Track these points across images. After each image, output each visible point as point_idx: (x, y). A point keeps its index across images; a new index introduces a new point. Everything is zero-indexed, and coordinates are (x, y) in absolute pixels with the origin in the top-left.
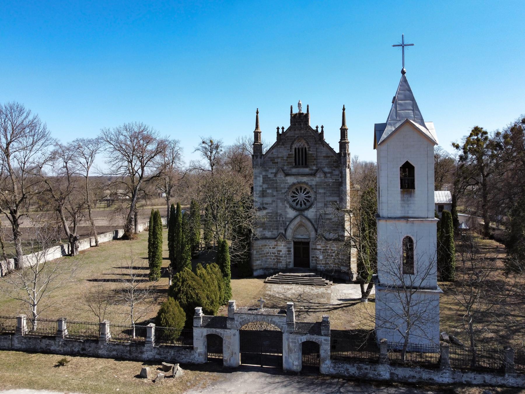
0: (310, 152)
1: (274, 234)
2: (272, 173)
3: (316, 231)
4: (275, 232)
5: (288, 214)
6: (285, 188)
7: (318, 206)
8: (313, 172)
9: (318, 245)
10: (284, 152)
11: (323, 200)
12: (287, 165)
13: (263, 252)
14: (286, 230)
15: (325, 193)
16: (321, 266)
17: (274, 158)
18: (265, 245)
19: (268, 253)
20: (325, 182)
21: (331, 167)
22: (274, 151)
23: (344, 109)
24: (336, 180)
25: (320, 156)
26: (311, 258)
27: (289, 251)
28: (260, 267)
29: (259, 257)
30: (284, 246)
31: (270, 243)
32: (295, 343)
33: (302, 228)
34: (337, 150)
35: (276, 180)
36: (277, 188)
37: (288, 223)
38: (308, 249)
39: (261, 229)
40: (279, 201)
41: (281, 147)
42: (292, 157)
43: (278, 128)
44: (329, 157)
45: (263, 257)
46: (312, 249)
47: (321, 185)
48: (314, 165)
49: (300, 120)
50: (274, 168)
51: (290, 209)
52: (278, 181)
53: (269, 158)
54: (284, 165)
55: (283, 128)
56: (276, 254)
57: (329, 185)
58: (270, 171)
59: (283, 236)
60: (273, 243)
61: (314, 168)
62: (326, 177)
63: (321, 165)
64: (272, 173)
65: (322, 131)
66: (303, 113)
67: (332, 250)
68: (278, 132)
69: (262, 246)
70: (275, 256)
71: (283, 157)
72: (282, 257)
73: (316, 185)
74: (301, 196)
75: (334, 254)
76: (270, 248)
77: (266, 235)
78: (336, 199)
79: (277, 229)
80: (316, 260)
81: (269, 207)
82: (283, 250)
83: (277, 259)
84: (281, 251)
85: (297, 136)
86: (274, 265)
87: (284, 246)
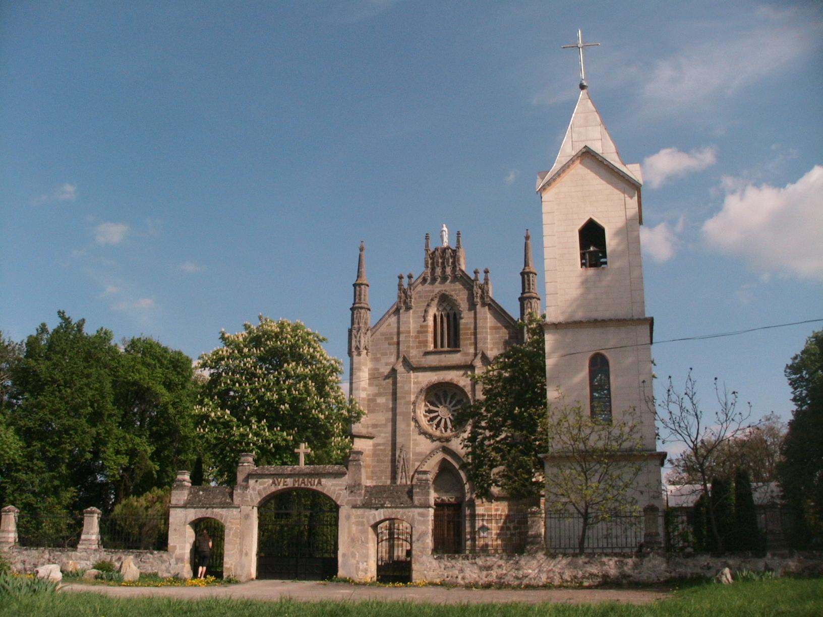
2: (387, 364)
32: (362, 524)
43: (401, 277)
48: (471, 344)
49: (442, 262)
53: (382, 334)
55: (410, 277)
58: (384, 360)
64: (387, 364)
65: (486, 280)
66: (448, 248)
68: (400, 285)
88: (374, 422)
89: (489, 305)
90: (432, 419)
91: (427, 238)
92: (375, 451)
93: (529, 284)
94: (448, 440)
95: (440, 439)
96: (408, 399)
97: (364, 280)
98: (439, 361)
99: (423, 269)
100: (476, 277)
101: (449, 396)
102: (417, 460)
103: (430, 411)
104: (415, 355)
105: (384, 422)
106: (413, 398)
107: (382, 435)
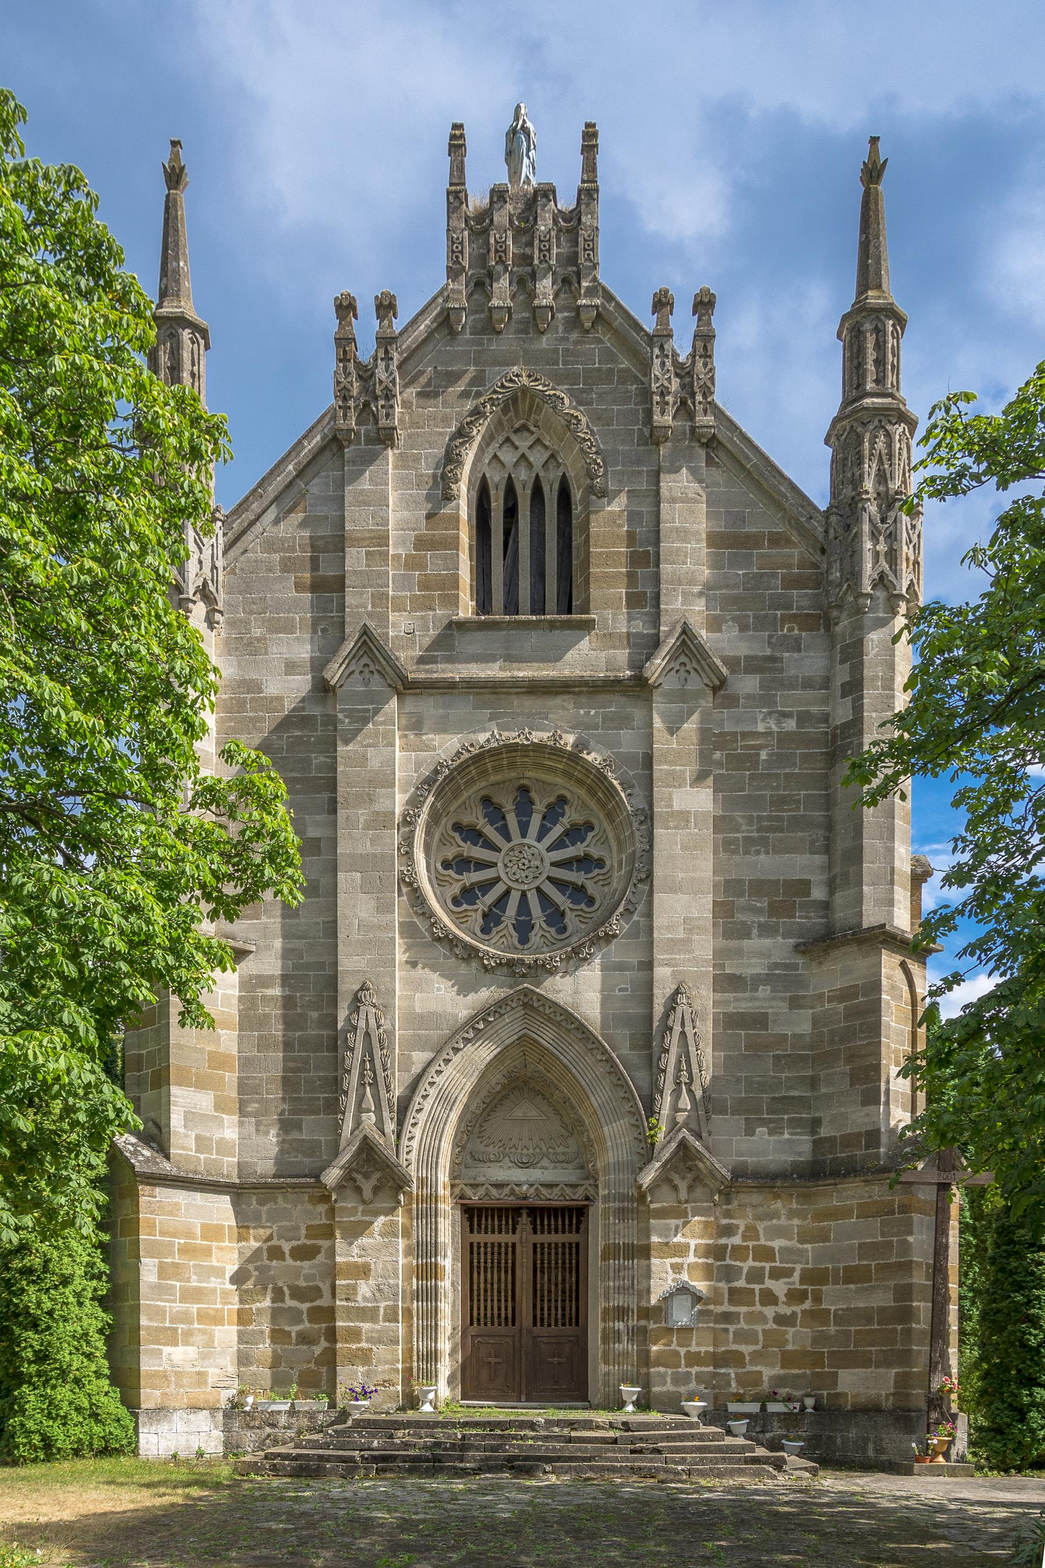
24: (803, 718)
26: (596, 1326)
38: (574, 1259)
46: (611, 1252)
62: (732, 701)
66: (547, 192)
72: (370, 1314)
78: (804, 865)
87: (390, 1232)
89: (712, 444)
93: (880, 362)
94: (541, 970)
96: (380, 806)
97: (187, 307)
99: (442, 279)
100: (663, 322)
106: (399, 802)
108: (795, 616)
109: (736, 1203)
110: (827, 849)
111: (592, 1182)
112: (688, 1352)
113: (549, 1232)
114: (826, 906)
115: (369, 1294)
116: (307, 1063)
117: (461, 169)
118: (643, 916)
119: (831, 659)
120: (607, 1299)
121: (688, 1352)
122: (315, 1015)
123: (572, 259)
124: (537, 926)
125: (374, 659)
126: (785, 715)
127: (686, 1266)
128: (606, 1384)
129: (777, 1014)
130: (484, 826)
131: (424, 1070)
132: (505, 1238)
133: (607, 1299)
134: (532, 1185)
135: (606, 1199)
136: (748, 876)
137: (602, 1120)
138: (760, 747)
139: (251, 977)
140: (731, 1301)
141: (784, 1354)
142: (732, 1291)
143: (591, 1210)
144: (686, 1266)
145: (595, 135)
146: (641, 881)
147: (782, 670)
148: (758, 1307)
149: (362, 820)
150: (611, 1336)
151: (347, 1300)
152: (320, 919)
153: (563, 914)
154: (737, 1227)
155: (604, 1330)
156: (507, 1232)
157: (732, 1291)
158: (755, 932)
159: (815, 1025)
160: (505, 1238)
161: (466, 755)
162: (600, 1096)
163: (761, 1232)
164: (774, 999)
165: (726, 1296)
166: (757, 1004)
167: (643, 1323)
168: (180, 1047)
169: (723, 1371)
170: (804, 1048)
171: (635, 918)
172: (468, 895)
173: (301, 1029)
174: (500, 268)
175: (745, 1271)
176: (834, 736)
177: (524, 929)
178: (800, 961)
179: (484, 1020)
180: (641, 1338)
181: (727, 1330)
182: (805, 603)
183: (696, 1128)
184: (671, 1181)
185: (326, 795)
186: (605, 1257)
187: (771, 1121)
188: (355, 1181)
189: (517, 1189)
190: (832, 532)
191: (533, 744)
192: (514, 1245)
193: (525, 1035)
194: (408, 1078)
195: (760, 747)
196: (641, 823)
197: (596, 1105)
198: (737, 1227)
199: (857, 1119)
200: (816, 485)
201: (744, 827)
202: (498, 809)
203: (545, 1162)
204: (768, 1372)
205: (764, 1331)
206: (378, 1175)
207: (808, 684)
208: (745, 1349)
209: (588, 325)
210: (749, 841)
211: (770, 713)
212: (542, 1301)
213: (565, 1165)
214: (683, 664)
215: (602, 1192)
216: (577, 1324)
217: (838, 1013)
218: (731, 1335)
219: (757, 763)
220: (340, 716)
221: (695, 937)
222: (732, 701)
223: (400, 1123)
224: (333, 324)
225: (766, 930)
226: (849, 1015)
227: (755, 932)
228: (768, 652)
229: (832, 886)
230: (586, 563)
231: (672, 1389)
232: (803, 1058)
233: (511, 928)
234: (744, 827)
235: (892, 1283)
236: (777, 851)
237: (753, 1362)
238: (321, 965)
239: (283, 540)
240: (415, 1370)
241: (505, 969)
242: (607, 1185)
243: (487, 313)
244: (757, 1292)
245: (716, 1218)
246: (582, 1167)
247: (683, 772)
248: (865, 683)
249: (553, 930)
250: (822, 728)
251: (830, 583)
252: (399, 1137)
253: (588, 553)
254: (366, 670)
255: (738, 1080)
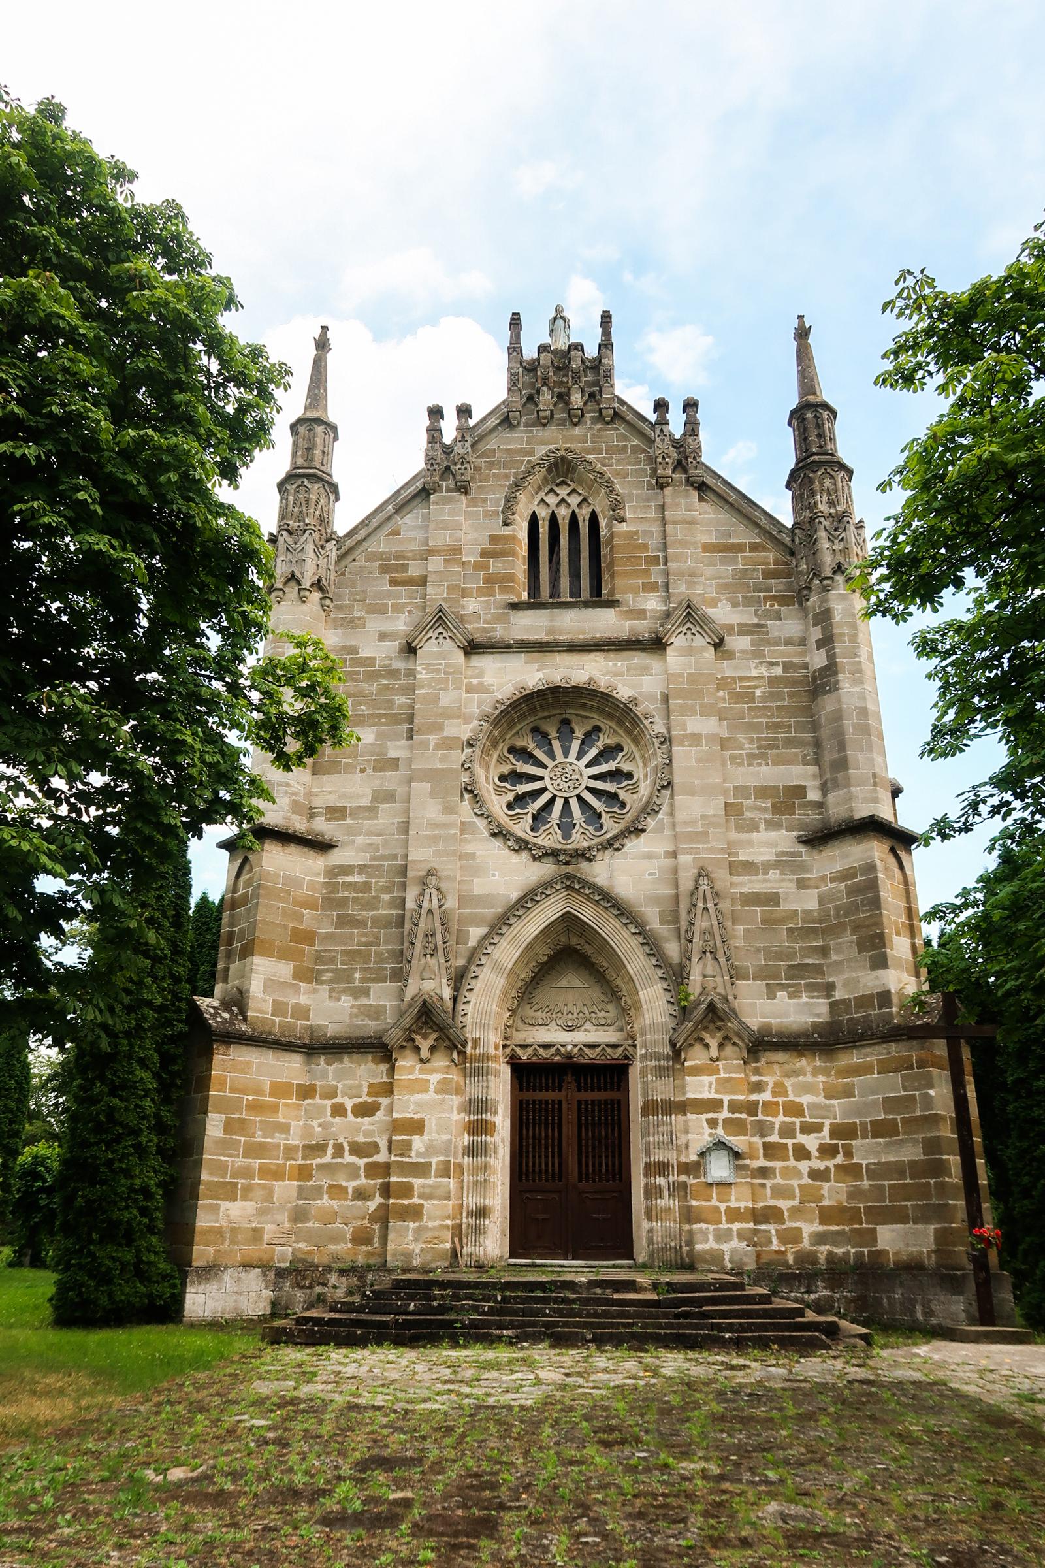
0: (623, 527)
1: (376, 1013)
2: (383, 637)
3: (676, 976)
4: (382, 996)
5: (477, 871)
6: (467, 720)
7: (681, 816)
8: (644, 628)
9: (697, 1071)
10: (465, 524)
11: (716, 779)
12: (482, 592)
13: (278, 1139)
14: (459, 979)
15: (724, 744)
16: (723, 1236)
17: (399, 556)
18: (306, 1092)
19: (320, 1148)
20: (723, 683)
21: (748, 602)
22: (408, 521)
23: (802, 333)
24: (787, 666)
25: (684, 544)
27: (480, 1128)
28: (253, 1251)
29: (247, 1173)
30: (444, 1088)
31: (339, 1076)
33: (572, 979)
34: (787, 518)
35: (411, 673)
36: (410, 719)
37: (476, 933)
39: (284, 970)
40: (421, 788)
41: (449, 501)
42: (512, 553)
43: (436, 413)
44: (739, 548)
45: (278, 1175)
46: (649, 1108)
47: (699, 694)
48: (651, 588)
49: (561, 381)
50: (397, 609)
51: (497, 843)
52: (422, 674)
53: (372, 557)
54: (464, 593)
55: (464, 411)
56: (381, 1157)
57: (748, 696)
58: (375, 624)
59: (433, 1026)
60: (363, 1073)
61: (653, 604)
62: (730, 655)
63: (691, 584)
64: (383, 637)
65: (692, 427)
66: (579, 347)
67: (795, 1109)
68: (434, 434)
69: (280, 1090)
70: (374, 1170)
71: (458, 551)
72: (421, 1169)
73: (666, 698)
74: (568, 771)
75: (811, 1142)
76: (339, 1110)
77: (315, 1020)
78: (801, 774)
79: (400, 976)
80: (680, 1190)
81: (351, 831)
82: (431, 1123)
83: (386, 1190)
84: (417, 1127)
85: (541, 450)
86: (361, 1238)
87: (444, 1088)
88: (332, 800)
90: (521, 800)
91: (515, 322)
92: (332, 887)
95: (551, 854)
98: (551, 631)
101: (579, 733)
102: (476, 921)
103: (516, 777)
104: (479, 612)
105: (366, 802)
107: (360, 840)
108: (774, 598)
109: (763, 1060)
110: (817, 762)
111: (630, 1042)
112: (728, 1207)
113: (593, 1090)
114: (820, 805)
115: (422, 1150)
116: (378, 938)
117: (518, 336)
118: (667, 814)
119: (807, 625)
120: (648, 1153)
121: (728, 1207)
122: (386, 897)
123: (596, 383)
124: (578, 826)
125: (447, 628)
126: (772, 664)
127: (721, 1122)
128: (650, 1241)
129: (787, 893)
130: (534, 749)
131: (479, 942)
132: (551, 1095)
133: (648, 1153)
134: (575, 1046)
135: (644, 1057)
136: (753, 782)
137: (638, 985)
138: (755, 687)
139: (335, 867)
140: (765, 1156)
141: (822, 1210)
142: (764, 1144)
143: (631, 1069)
144: (721, 1122)
145: (610, 317)
146: (663, 787)
147: (767, 633)
148: (792, 1162)
149: (432, 743)
150: (652, 1192)
151: (401, 1155)
152: (395, 821)
153: (599, 816)
154: (767, 1083)
155: (646, 1184)
156: (553, 1091)
157: (766, 1146)
158: (762, 826)
159: (821, 902)
160: (551, 1095)
161: (518, 695)
162: (636, 961)
163: (789, 1089)
164: (783, 880)
165: (761, 1151)
166: (769, 885)
167: (683, 1178)
168: (266, 922)
169: (763, 1227)
170: (813, 922)
171: (660, 816)
172: (521, 800)
173: (374, 909)
174: (545, 389)
175: (777, 1126)
176: (814, 678)
177: (566, 827)
178: (802, 849)
179: (532, 900)
180: (682, 1193)
181: (764, 1185)
182: (782, 587)
183: (723, 992)
184: (702, 1040)
185: (405, 726)
186: (645, 1113)
187: (789, 986)
188: (414, 1041)
189: (562, 1049)
190: (797, 541)
191: (573, 687)
192: (560, 1102)
193: (568, 912)
194: (464, 950)
195: (755, 687)
196: (662, 743)
197: (631, 972)
198: (767, 1083)
199: (869, 981)
200: (787, 518)
201: (746, 746)
202: (545, 735)
203: (588, 1026)
204: (809, 1228)
205: (799, 1186)
206: (434, 1036)
207: (789, 642)
208: (784, 1204)
209: (608, 419)
210: (751, 756)
211: (761, 663)
212: (587, 1157)
213: (606, 1028)
214: (689, 629)
215: (640, 1051)
216: (621, 1180)
217: (840, 891)
218: (768, 1191)
219: (754, 698)
220: (419, 669)
221: (711, 830)
222: (730, 655)
223: (456, 989)
224: (426, 422)
225: (771, 825)
226: (851, 891)
227: (762, 826)
228: (756, 621)
229: (824, 789)
230: (612, 564)
231: (715, 1246)
232: (814, 931)
233: (556, 827)
234: (746, 746)
235: (920, 1137)
236: (776, 764)
237: (792, 1219)
238: (395, 857)
239: (383, 553)
240: (464, 1226)
241: (551, 859)
242: (644, 1045)
243: (535, 415)
244: (790, 1147)
245: (746, 1075)
246: (621, 1030)
247: (693, 705)
248: (836, 638)
249: (591, 829)
250: (804, 672)
251: (801, 572)
252: (455, 999)
253: (613, 559)
254: (441, 637)
255: (758, 950)
